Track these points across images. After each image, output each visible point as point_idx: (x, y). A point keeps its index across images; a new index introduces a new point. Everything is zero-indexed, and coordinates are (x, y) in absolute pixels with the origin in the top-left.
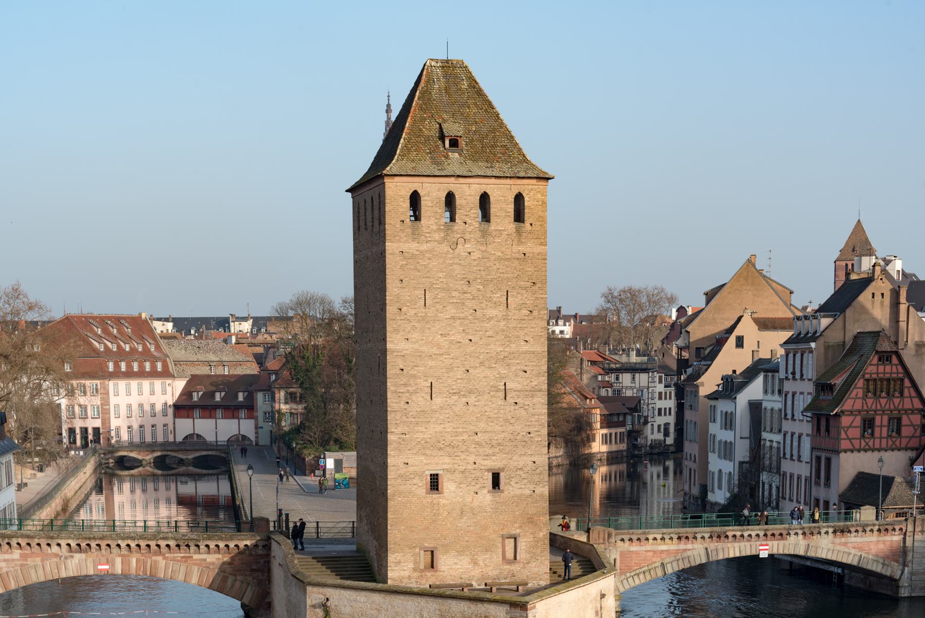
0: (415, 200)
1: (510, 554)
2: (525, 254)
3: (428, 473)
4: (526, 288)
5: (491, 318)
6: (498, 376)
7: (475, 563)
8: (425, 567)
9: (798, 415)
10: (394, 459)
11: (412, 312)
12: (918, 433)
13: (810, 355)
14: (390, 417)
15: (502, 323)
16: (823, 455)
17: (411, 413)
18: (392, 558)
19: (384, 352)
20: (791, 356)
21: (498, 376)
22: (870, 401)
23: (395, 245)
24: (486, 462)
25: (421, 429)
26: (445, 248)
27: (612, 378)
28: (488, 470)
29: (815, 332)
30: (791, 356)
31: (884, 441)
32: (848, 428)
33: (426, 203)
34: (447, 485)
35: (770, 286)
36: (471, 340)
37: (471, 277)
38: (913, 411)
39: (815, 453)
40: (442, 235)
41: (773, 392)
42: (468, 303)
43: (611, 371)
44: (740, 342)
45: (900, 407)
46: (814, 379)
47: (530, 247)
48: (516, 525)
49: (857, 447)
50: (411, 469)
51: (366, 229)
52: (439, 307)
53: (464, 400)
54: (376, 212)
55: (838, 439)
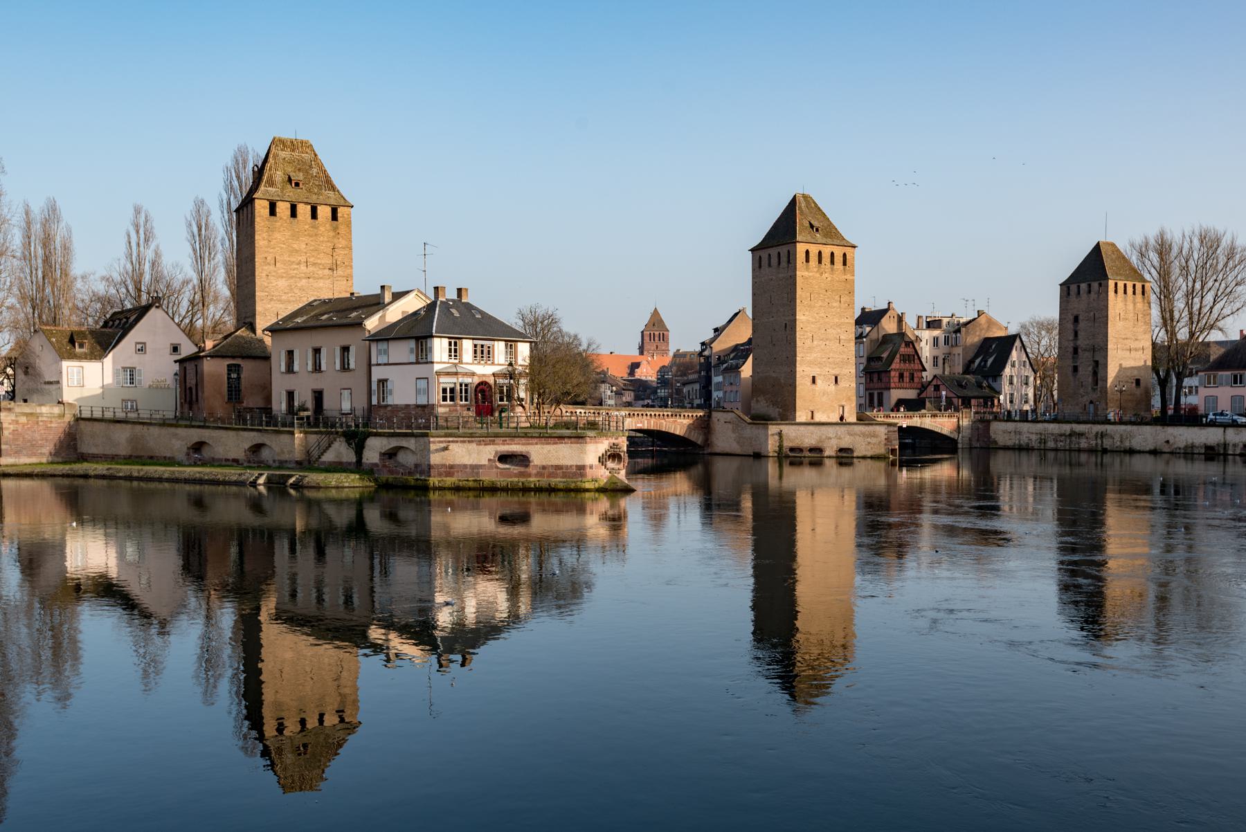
0: (807, 252)
7: (829, 417)
10: (799, 369)
13: (862, 345)
18: (798, 414)
19: (795, 320)
26: (818, 275)
29: (862, 333)
33: (811, 255)
34: (818, 381)
38: (918, 370)
46: (865, 356)
47: (848, 277)
50: (805, 373)
51: (770, 265)
55: (890, 382)
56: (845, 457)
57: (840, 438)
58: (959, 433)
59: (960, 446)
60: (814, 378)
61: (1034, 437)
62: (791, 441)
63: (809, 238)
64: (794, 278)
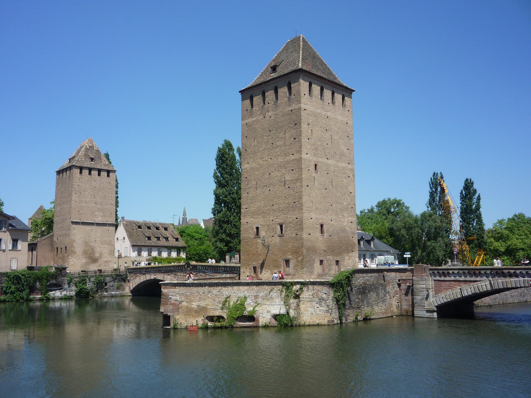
2: (292, 111)
3: (255, 227)
5: (279, 146)
6: (282, 174)
11: (250, 150)
15: (283, 148)
17: (249, 198)
21: (282, 174)
23: (244, 121)
25: (253, 205)
26: (262, 117)
28: (278, 224)
34: (262, 233)
36: (271, 159)
48: (290, 253)
50: (249, 225)
60: (257, 228)
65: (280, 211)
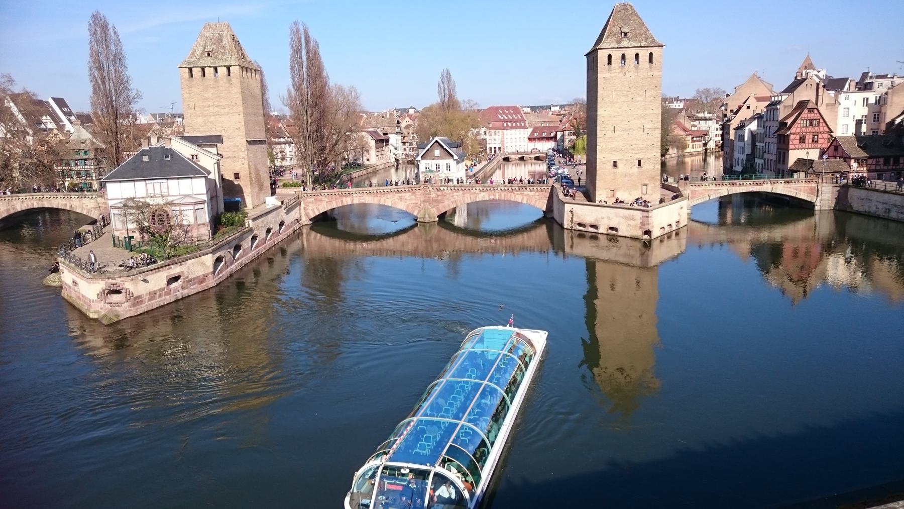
0: (610, 57)
1: (644, 192)
4: (653, 89)
7: (630, 194)
8: (611, 196)
9: (771, 135)
11: (607, 100)
12: (826, 142)
14: (598, 140)
16: (782, 151)
18: (598, 193)
19: (596, 116)
20: (769, 111)
22: (804, 129)
24: (635, 156)
25: (610, 144)
26: (621, 75)
27: (696, 123)
30: (769, 111)
31: (810, 145)
32: (793, 140)
33: (613, 59)
35: (763, 83)
37: (631, 86)
39: (778, 151)
40: (620, 70)
41: (761, 126)
42: (629, 95)
43: (697, 120)
44: (748, 108)
45: (818, 131)
47: (655, 73)
49: (797, 147)
50: (606, 159)
52: (618, 97)
53: (627, 133)
54: (595, 63)
55: (788, 144)
56: (613, 236)
57: (609, 218)
58: (817, 196)
59: (817, 208)
61: (880, 206)
62: (579, 217)
63: (614, 45)
64: (597, 78)
65: (638, 150)
